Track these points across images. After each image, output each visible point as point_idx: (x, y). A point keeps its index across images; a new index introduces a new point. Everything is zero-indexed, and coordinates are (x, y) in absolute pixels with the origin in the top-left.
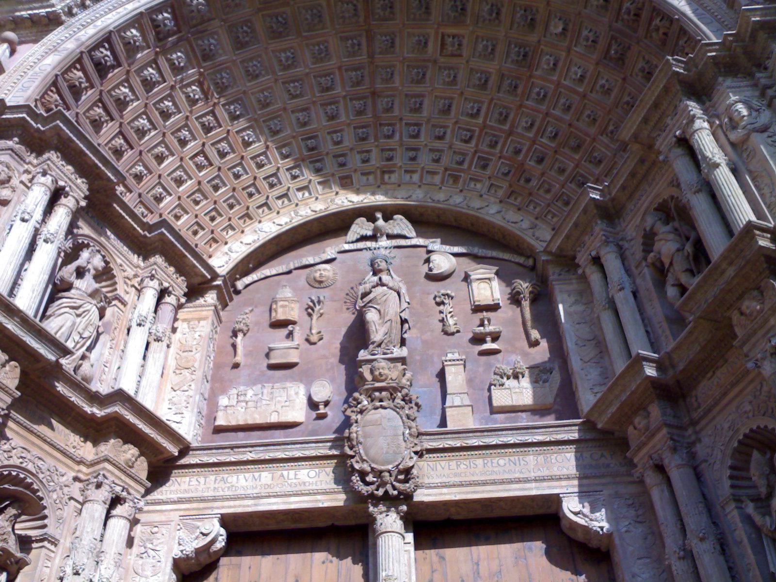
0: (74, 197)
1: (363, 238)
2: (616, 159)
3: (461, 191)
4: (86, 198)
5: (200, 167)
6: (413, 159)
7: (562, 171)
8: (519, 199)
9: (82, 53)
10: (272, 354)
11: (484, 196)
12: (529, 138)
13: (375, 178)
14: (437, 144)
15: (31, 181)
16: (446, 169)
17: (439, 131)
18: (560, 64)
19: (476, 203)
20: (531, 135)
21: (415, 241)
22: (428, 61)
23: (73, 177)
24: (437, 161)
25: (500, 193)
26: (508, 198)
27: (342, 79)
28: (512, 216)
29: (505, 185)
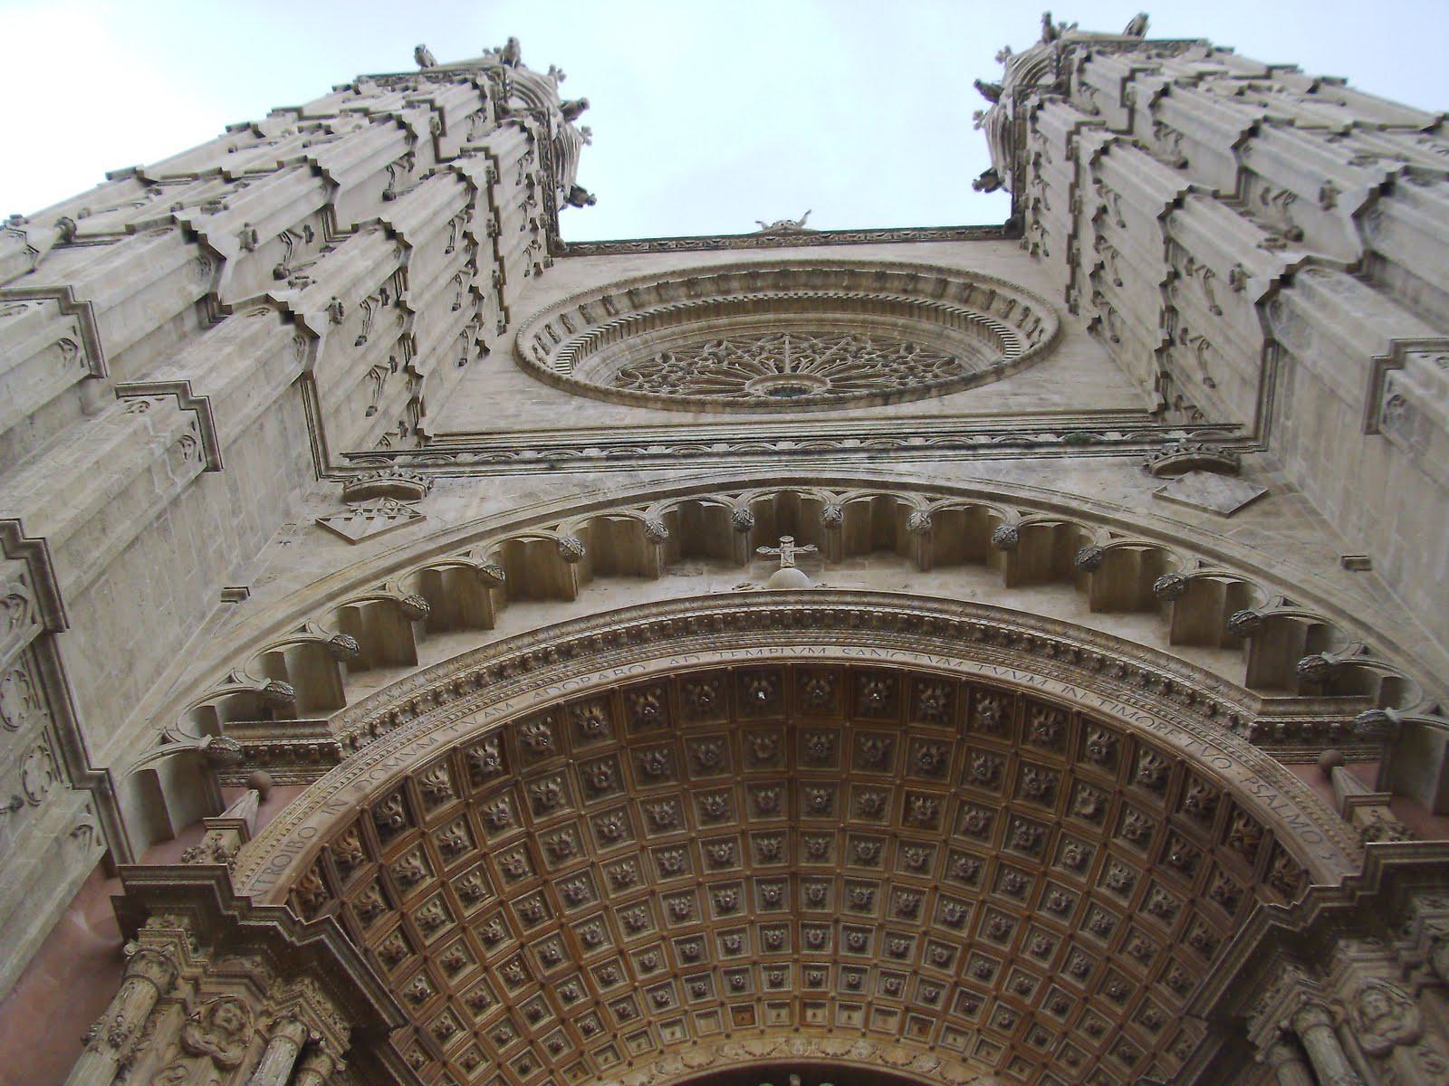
0: (330, 1057)
2: (1183, 1026)
3: (932, 1049)
4: (345, 1056)
5: (513, 983)
7: (1095, 1032)
8: (1027, 1072)
9: (363, 811)
11: (971, 1061)
12: (1042, 971)
13: (791, 1015)
14: (894, 965)
15: (271, 1028)
16: (907, 1009)
18: (1092, 861)
20: (1046, 965)
22: (884, 832)
23: (331, 1021)
24: (894, 993)
25: (996, 1057)
26: (1009, 1068)
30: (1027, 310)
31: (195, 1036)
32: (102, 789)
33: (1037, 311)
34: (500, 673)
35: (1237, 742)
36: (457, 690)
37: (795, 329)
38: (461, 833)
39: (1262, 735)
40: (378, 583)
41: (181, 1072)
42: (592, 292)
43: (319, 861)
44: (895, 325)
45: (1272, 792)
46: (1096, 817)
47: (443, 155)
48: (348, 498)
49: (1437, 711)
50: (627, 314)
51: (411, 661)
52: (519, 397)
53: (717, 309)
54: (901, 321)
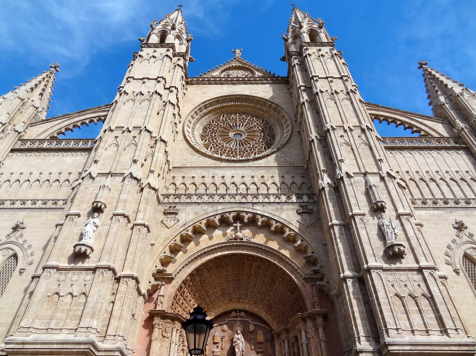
1: (234, 317)
6: (247, 296)
10: (214, 353)
14: (252, 294)
16: (254, 300)
17: (253, 291)
19: (260, 311)
21: (245, 319)
25: (266, 309)
28: (268, 317)
29: (267, 308)
31: (164, 334)
32: (144, 296)
35: (301, 278)
36: (189, 262)
39: (305, 279)
40: (174, 239)
41: (163, 340)
42: (197, 107)
43: (174, 298)
45: (304, 288)
47: (166, 87)
49: (328, 283)
52: (186, 151)
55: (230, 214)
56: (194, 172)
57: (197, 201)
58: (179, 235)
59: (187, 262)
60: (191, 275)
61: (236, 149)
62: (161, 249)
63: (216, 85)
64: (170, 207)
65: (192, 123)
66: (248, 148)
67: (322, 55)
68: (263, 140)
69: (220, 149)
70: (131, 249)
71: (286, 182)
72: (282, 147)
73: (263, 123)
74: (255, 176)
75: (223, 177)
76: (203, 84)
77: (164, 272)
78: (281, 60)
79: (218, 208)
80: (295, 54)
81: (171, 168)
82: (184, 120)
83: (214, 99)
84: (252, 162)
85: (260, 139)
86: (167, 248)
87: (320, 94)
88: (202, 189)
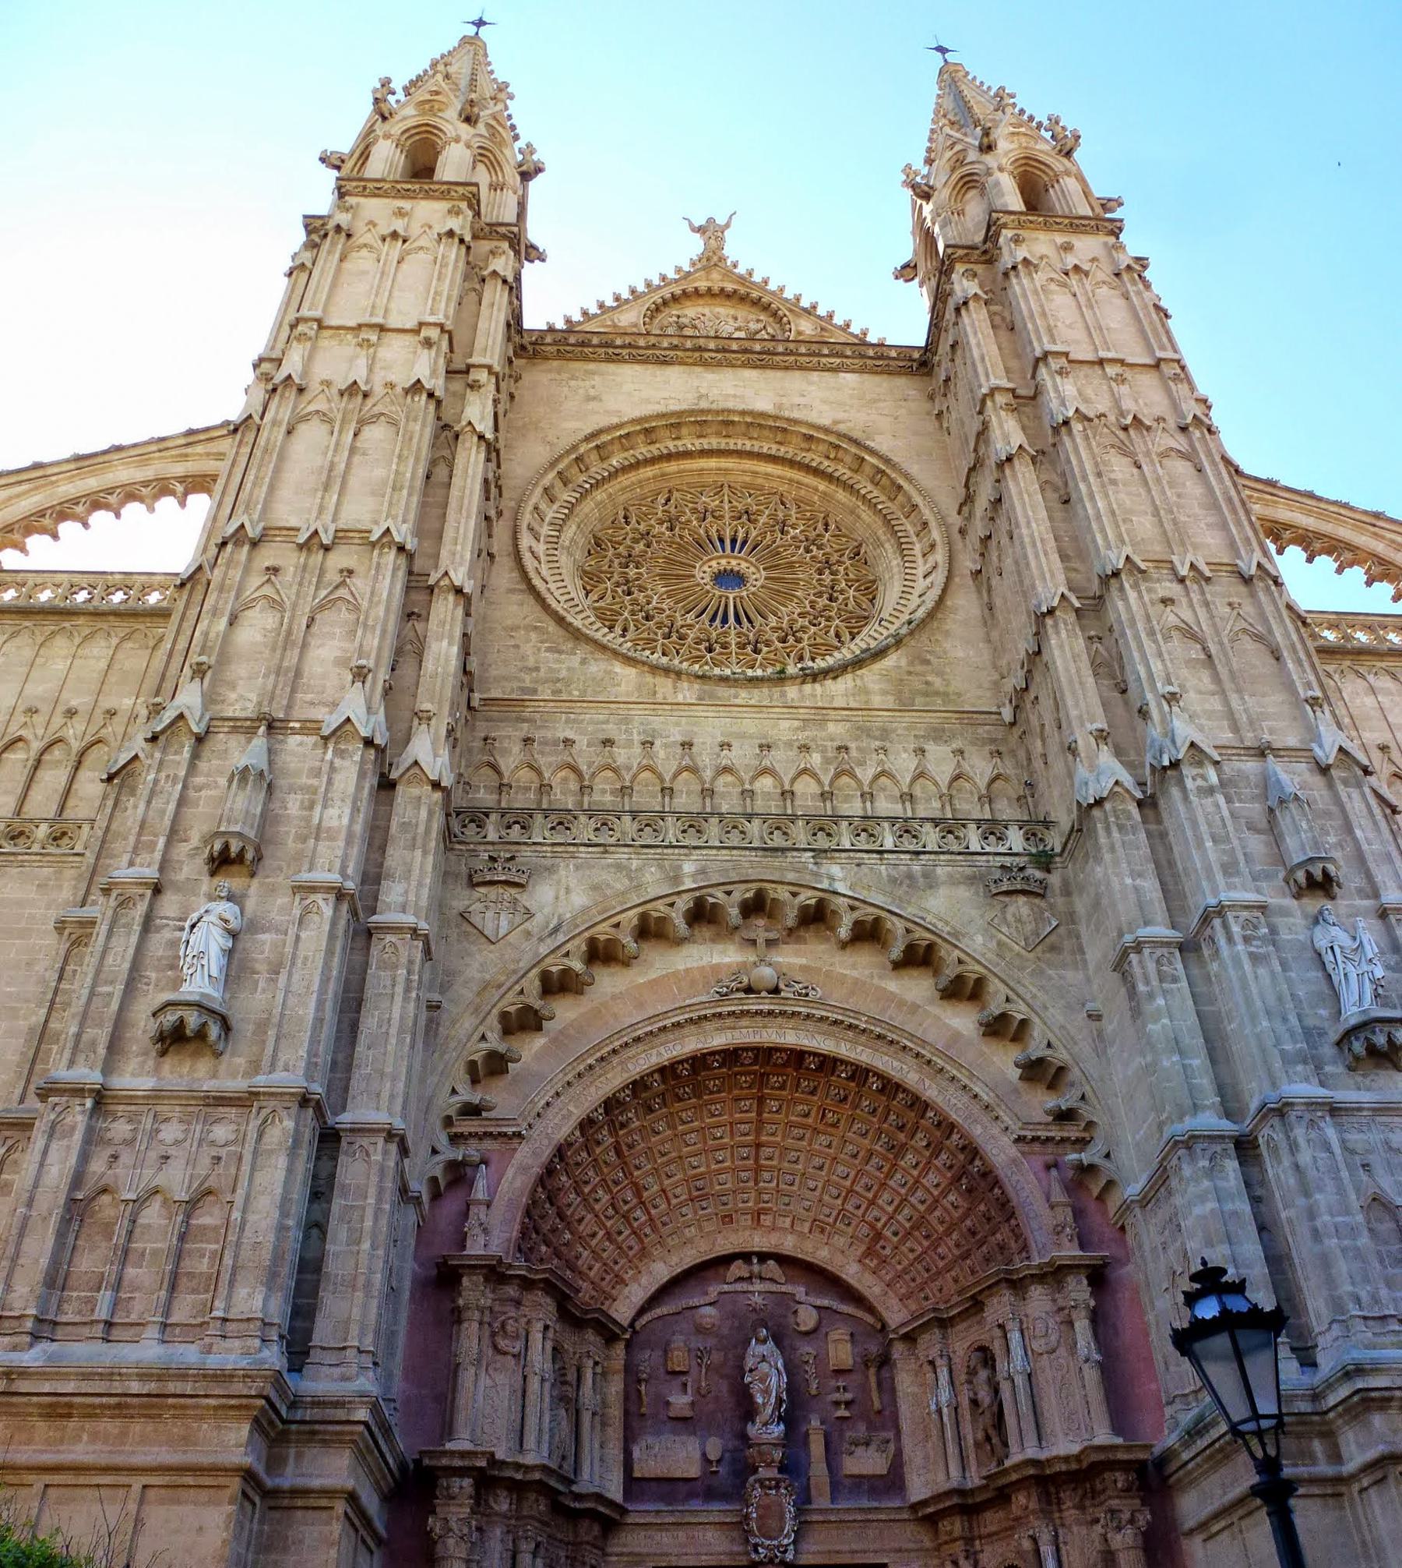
27: (732, 1131)
30: (925, 524)
33: (936, 534)
34: (602, 1059)
37: (732, 478)
38: (584, 1154)
40: (518, 988)
42: (568, 452)
44: (816, 490)
46: (928, 1145)
48: (473, 884)
50: (597, 469)
51: (539, 1028)
52: (533, 635)
53: (669, 457)
54: (822, 487)
55: (729, 893)
56: (567, 721)
57: (596, 840)
58: (535, 971)
59: (569, 1077)
60: (587, 1125)
61: (726, 634)
62: (468, 1023)
63: (637, 367)
64: (493, 859)
65: (547, 520)
66: (774, 629)
67: (1076, 268)
68: (831, 599)
69: (660, 632)
70: (369, 1023)
71: (931, 767)
72: (911, 633)
73: (826, 530)
74: (812, 745)
75: (687, 745)
76: (586, 359)
77: (484, 1114)
78: (897, 278)
79: (680, 867)
80: (967, 255)
81: (475, 703)
82: (513, 504)
83: (633, 421)
84: (795, 688)
85: (820, 595)
86: (493, 1020)
87: (1077, 427)
88: (604, 792)
